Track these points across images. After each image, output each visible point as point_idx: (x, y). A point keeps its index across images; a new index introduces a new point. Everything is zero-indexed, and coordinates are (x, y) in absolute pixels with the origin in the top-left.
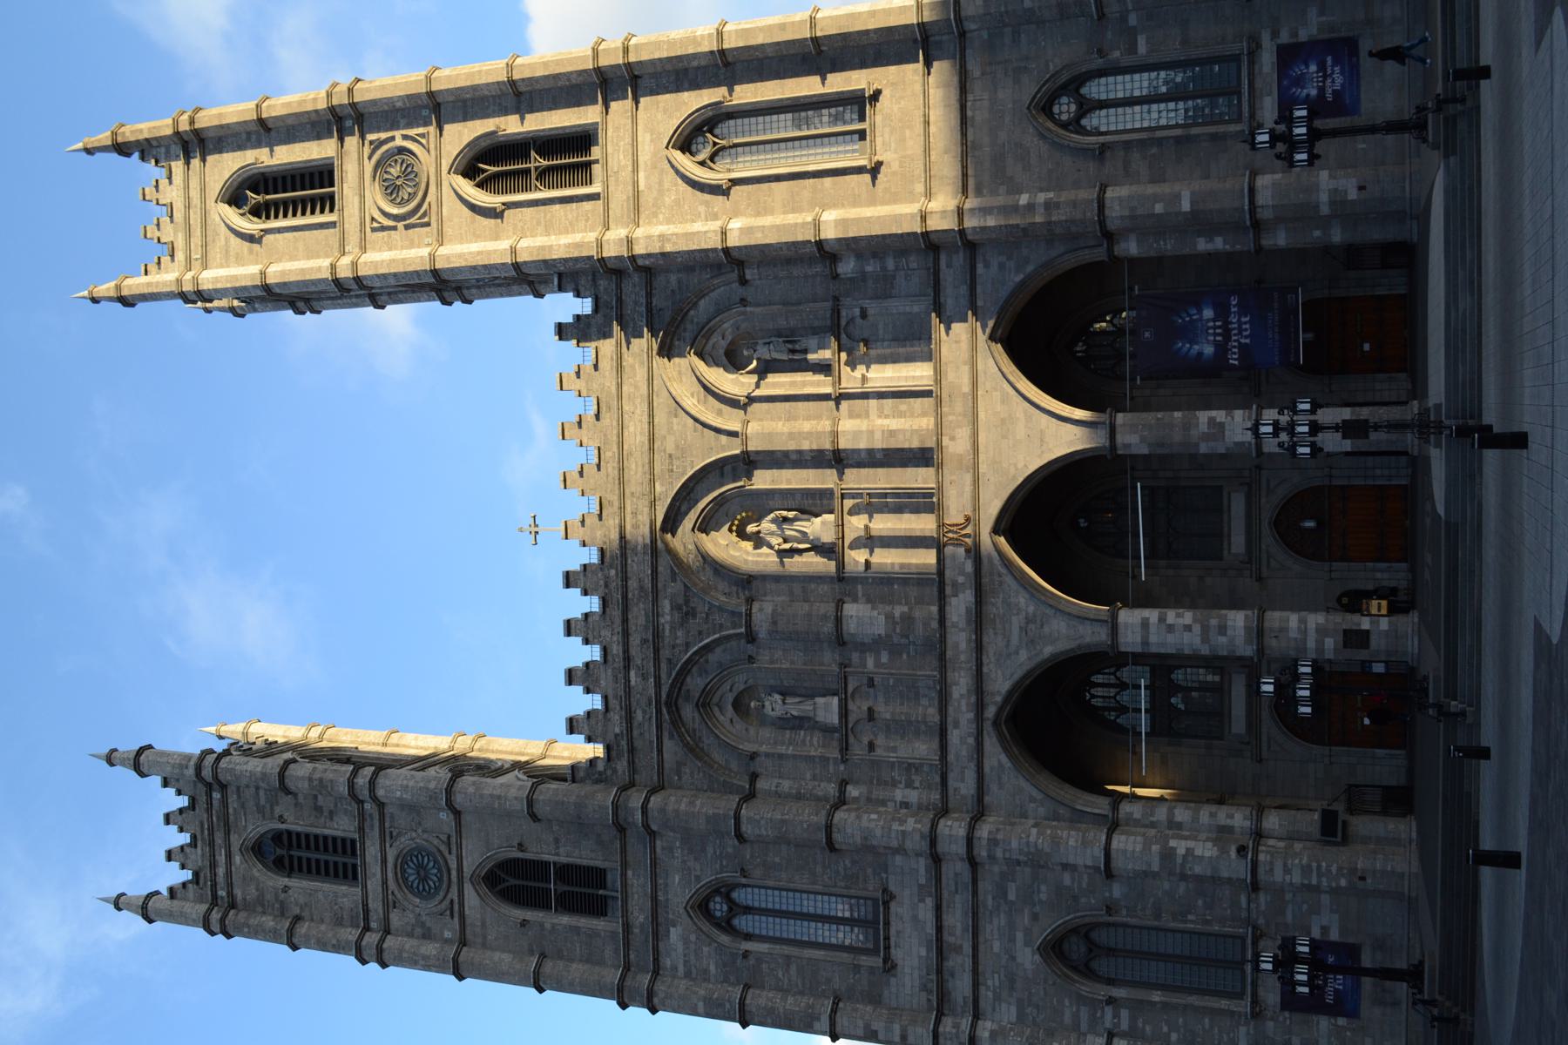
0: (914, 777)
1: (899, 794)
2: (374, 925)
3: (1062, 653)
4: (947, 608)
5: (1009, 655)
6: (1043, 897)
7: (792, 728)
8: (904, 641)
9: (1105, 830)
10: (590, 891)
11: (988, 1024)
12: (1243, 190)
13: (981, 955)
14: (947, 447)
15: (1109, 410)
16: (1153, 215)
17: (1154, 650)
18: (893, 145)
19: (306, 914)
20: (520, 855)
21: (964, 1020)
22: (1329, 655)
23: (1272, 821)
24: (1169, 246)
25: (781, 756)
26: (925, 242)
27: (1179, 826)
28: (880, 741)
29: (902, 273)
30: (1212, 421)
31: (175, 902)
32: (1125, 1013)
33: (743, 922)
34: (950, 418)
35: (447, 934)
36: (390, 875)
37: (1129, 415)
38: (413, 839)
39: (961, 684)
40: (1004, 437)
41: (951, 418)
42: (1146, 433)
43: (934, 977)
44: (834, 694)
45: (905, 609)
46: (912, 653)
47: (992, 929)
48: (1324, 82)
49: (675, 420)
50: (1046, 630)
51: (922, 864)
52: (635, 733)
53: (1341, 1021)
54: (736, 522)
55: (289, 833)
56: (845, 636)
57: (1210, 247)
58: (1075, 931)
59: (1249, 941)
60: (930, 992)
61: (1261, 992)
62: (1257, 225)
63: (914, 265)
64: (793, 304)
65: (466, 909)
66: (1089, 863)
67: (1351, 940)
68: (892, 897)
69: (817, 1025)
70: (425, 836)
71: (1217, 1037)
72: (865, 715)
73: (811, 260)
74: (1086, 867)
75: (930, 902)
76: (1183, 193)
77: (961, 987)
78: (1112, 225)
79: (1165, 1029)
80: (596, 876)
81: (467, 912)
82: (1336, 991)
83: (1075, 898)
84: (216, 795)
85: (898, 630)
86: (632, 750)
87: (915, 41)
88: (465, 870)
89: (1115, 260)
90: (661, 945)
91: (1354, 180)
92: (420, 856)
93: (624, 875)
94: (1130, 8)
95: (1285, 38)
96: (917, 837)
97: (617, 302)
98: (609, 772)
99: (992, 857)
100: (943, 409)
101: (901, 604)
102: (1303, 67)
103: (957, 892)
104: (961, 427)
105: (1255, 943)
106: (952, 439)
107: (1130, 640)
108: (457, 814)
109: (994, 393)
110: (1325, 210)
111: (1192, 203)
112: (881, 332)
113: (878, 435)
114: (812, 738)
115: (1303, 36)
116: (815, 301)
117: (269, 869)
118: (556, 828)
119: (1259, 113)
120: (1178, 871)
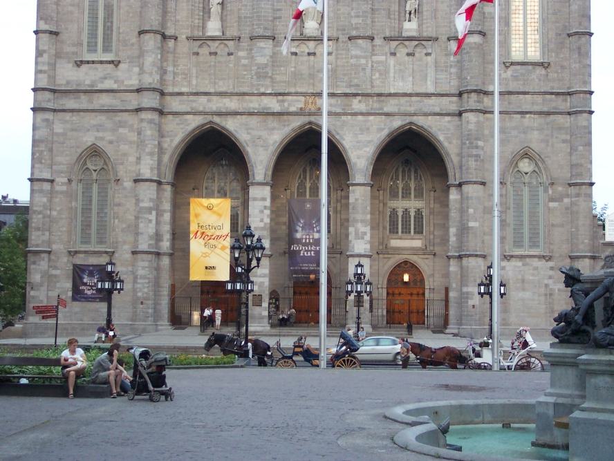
0: (180, 77)
3: (249, 158)
5: (247, 129)
7: (204, 8)
12: (476, 251)
15: (372, 183)
16: (468, 208)
17: (250, 203)
21: (52, 105)
23: (166, 261)
24: (454, 214)
26: (463, 91)
27: (162, 215)
28: (201, 58)
29: (449, 76)
30: (365, 233)
32: (64, 188)
34: (371, 100)
37: (369, 193)
39: (231, 104)
40: (361, 129)
42: (360, 201)
43: (74, 87)
44: (223, 34)
46: (246, 76)
47: (102, 118)
50: (261, 149)
51: (133, 82)
53: (70, 294)
58: (105, 163)
62: (460, 257)
63: (452, 84)
64: (435, 15)
66: (141, 171)
68: (116, 66)
69: (42, 23)
72: (212, 51)
74: (139, 170)
75: (115, 87)
76: (478, 223)
77: (70, 103)
79: (58, 209)
89: (448, 187)
91: (478, 303)
96: (150, 80)
99: (142, 120)
100: (375, 98)
101: (273, 70)
103: (122, 101)
106: (360, 102)
107: (254, 192)
110: (465, 289)
111: (472, 227)
112: (418, 63)
113: (363, 61)
114: (199, 19)
116: (436, 27)
119: (514, 259)
120: (140, 215)
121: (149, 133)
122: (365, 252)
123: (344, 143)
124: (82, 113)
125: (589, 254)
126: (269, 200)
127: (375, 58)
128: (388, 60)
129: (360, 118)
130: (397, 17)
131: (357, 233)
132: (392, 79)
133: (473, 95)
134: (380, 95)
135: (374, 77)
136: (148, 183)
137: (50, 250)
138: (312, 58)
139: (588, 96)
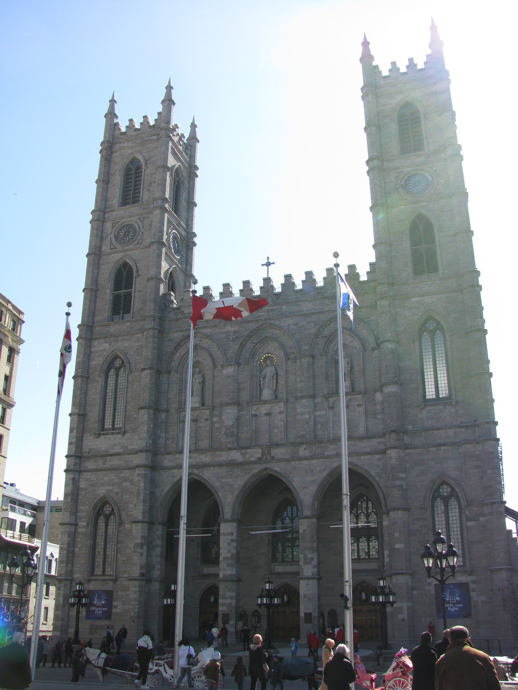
0: (170, 440)
1: (163, 435)
2: (106, 216)
4: (235, 451)
6: (125, 496)
8: (223, 433)
9: (149, 521)
10: (122, 308)
11: (77, 477)
13: (103, 472)
14: (301, 447)
17: (222, 538)
18: (429, 414)
19: (110, 185)
20: (134, 276)
22: (221, 608)
25: (177, 383)
30: (312, 559)
31: (112, 127)
33: (112, 372)
34: (314, 448)
35: (103, 248)
36: (126, 220)
38: (139, 228)
41: (314, 448)
44: (203, 405)
45: (236, 433)
46: (219, 437)
48: (452, 603)
49: (313, 324)
52: (184, 320)
54: (272, 356)
55: (141, 172)
56: (225, 408)
57: (385, 556)
59: (112, 578)
60: (89, 453)
61: (93, 582)
65: (114, 255)
67: (113, 616)
70: (141, 233)
71: (77, 566)
73: (380, 380)
75: (122, 450)
77: (90, 465)
78: (391, 513)
79: (79, 546)
80: (127, 310)
81: (113, 255)
82: (95, 611)
83: (124, 510)
84: (155, 138)
85: (227, 431)
86: (177, 320)
87: (475, 421)
88: (128, 252)
90: (102, 340)
92: (133, 232)
93: (128, 321)
94: (488, 517)
95: (472, 586)
96: (144, 444)
97: (364, 292)
98: (169, 310)
102: (458, 594)
103: (125, 461)
104: (310, 452)
105: (110, 580)
106: (305, 449)
108: (149, 246)
109: (324, 466)
111: (399, 548)
113: (307, 416)
115: (473, 594)
117: (128, 165)
118: (145, 290)
121: (142, 485)
122: (313, 575)
123: (293, 483)
124: (98, 472)
125: (505, 567)
126: (235, 534)
127: (317, 413)
128: (328, 414)
129: (305, 462)
130: (334, 378)
131: (305, 557)
132: (331, 428)
133: (393, 436)
134: (321, 442)
135: (317, 429)
136: (140, 524)
137: (71, 578)
138: (268, 417)
139: (492, 426)
